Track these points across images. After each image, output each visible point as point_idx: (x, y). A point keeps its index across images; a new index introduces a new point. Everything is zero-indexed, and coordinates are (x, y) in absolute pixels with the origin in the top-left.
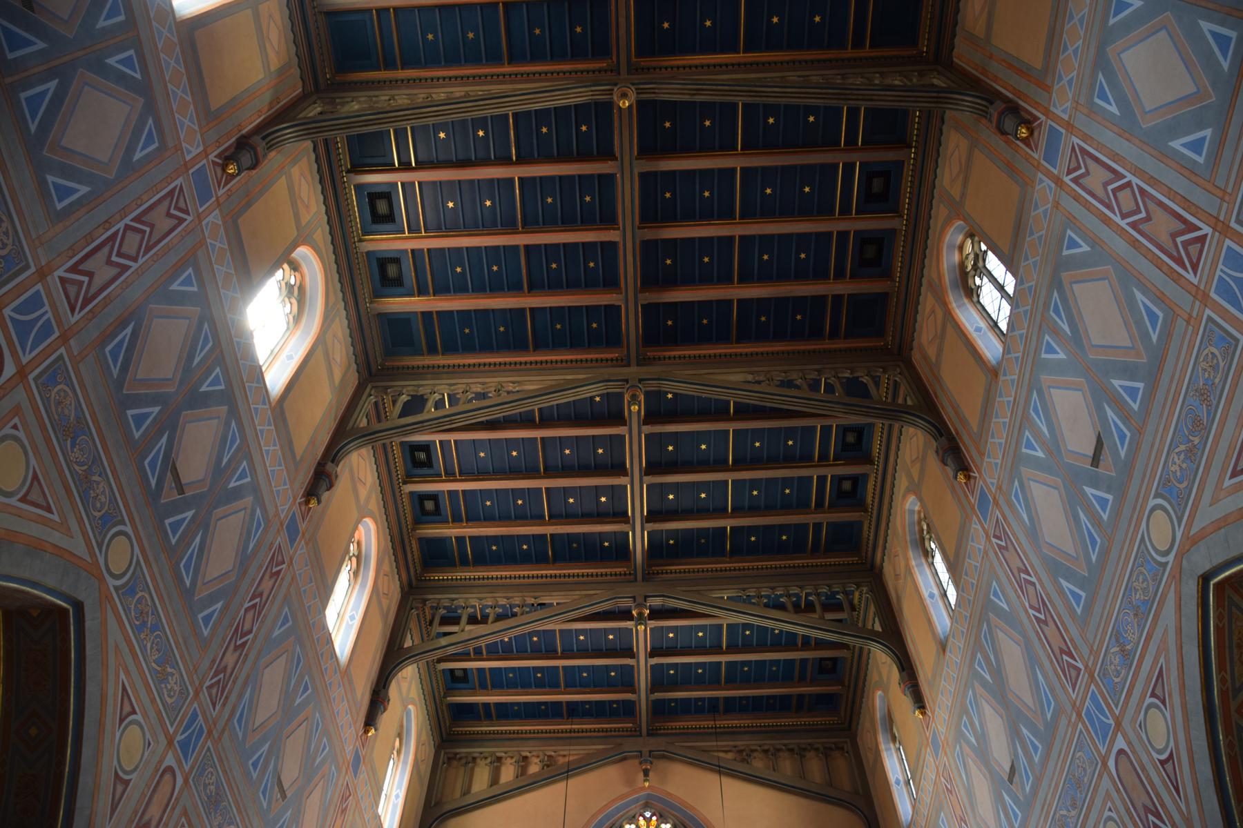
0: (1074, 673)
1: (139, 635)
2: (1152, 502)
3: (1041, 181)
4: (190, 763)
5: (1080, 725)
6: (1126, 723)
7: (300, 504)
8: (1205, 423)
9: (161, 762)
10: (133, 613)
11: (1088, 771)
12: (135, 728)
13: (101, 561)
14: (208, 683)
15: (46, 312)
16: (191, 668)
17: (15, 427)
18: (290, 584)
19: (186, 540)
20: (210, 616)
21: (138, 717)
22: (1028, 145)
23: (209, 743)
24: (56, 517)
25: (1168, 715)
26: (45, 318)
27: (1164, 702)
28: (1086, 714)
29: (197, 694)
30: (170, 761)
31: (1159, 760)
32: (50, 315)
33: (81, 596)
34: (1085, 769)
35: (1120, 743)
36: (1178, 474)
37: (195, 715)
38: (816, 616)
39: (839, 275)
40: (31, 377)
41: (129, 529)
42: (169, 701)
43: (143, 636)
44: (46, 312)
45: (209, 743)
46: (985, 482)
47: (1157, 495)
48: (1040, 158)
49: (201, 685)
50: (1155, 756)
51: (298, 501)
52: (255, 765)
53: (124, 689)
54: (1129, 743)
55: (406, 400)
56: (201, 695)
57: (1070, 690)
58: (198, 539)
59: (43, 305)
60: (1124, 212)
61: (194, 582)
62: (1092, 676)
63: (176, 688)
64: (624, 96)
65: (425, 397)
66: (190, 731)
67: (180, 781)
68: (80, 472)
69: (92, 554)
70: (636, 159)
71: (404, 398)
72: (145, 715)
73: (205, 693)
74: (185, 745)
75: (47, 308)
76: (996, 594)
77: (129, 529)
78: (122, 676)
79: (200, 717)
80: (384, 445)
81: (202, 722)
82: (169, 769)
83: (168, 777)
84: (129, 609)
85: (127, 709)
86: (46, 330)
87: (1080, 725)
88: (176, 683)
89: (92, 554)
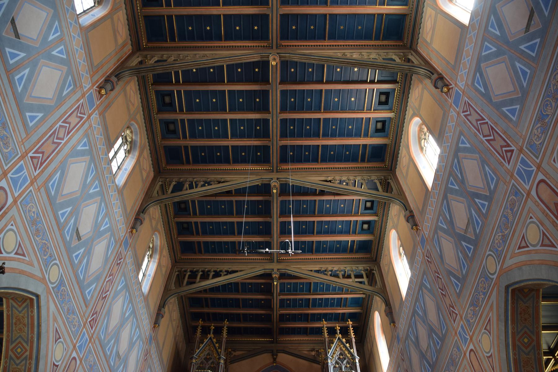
0: (455, 315)
1: (62, 305)
2: (488, 253)
3: (452, 112)
4: (82, 355)
5: (456, 337)
6: (474, 339)
7: (129, 232)
8: (509, 226)
9: (71, 355)
10: (59, 297)
11: (458, 356)
12: (61, 344)
13: (47, 277)
14: (89, 320)
15: (25, 172)
16: (82, 314)
17: (12, 225)
18: (124, 269)
19: (80, 262)
20: (90, 291)
21: (62, 340)
22: (447, 95)
23: (90, 344)
24: (27, 259)
25: (491, 338)
26: (25, 174)
27: (490, 333)
28: (459, 333)
29: (84, 325)
30: (74, 354)
31: (487, 356)
32: (26, 173)
33: (39, 293)
34: (457, 355)
35: (471, 347)
36: (498, 244)
37: (84, 334)
38: (350, 280)
39: (366, 135)
40: (19, 202)
41: (57, 262)
42: (73, 330)
43: (63, 305)
44: (25, 172)
45: (90, 344)
46: (424, 232)
47: (490, 250)
48: (451, 102)
49: (87, 321)
50: (485, 354)
51: (129, 231)
52: (109, 350)
53: (56, 329)
54: (475, 348)
55: (174, 184)
56: (87, 325)
57: (453, 322)
58: (85, 260)
59: (24, 170)
60: (487, 125)
61: (84, 277)
62: (461, 317)
63: (77, 324)
64: (274, 59)
65: (183, 183)
66: (82, 341)
67: (78, 362)
68: (38, 240)
69: (43, 273)
70: (279, 84)
71: (174, 183)
72: (65, 340)
73: (88, 324)
74: (80, 347)
75: (25, 170)
76: (425, 281)
77: (57, 262)
78: (56, 325)
79: (86, 334)
80: (165, 204)
81: (87, 336)
82: (74, 358)
83: (74, 361)
84: (58, 295)
85: (58, 337)
86: (25, 180)
87: (456, 337)
88: (76, 322)
89: (43, 273)
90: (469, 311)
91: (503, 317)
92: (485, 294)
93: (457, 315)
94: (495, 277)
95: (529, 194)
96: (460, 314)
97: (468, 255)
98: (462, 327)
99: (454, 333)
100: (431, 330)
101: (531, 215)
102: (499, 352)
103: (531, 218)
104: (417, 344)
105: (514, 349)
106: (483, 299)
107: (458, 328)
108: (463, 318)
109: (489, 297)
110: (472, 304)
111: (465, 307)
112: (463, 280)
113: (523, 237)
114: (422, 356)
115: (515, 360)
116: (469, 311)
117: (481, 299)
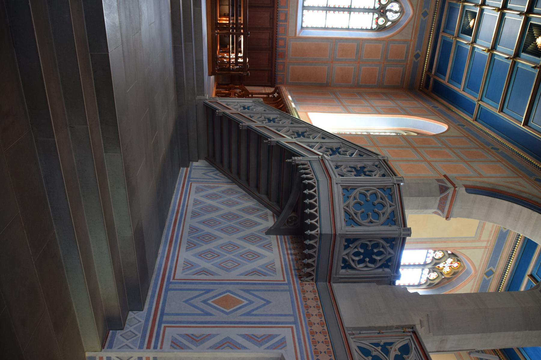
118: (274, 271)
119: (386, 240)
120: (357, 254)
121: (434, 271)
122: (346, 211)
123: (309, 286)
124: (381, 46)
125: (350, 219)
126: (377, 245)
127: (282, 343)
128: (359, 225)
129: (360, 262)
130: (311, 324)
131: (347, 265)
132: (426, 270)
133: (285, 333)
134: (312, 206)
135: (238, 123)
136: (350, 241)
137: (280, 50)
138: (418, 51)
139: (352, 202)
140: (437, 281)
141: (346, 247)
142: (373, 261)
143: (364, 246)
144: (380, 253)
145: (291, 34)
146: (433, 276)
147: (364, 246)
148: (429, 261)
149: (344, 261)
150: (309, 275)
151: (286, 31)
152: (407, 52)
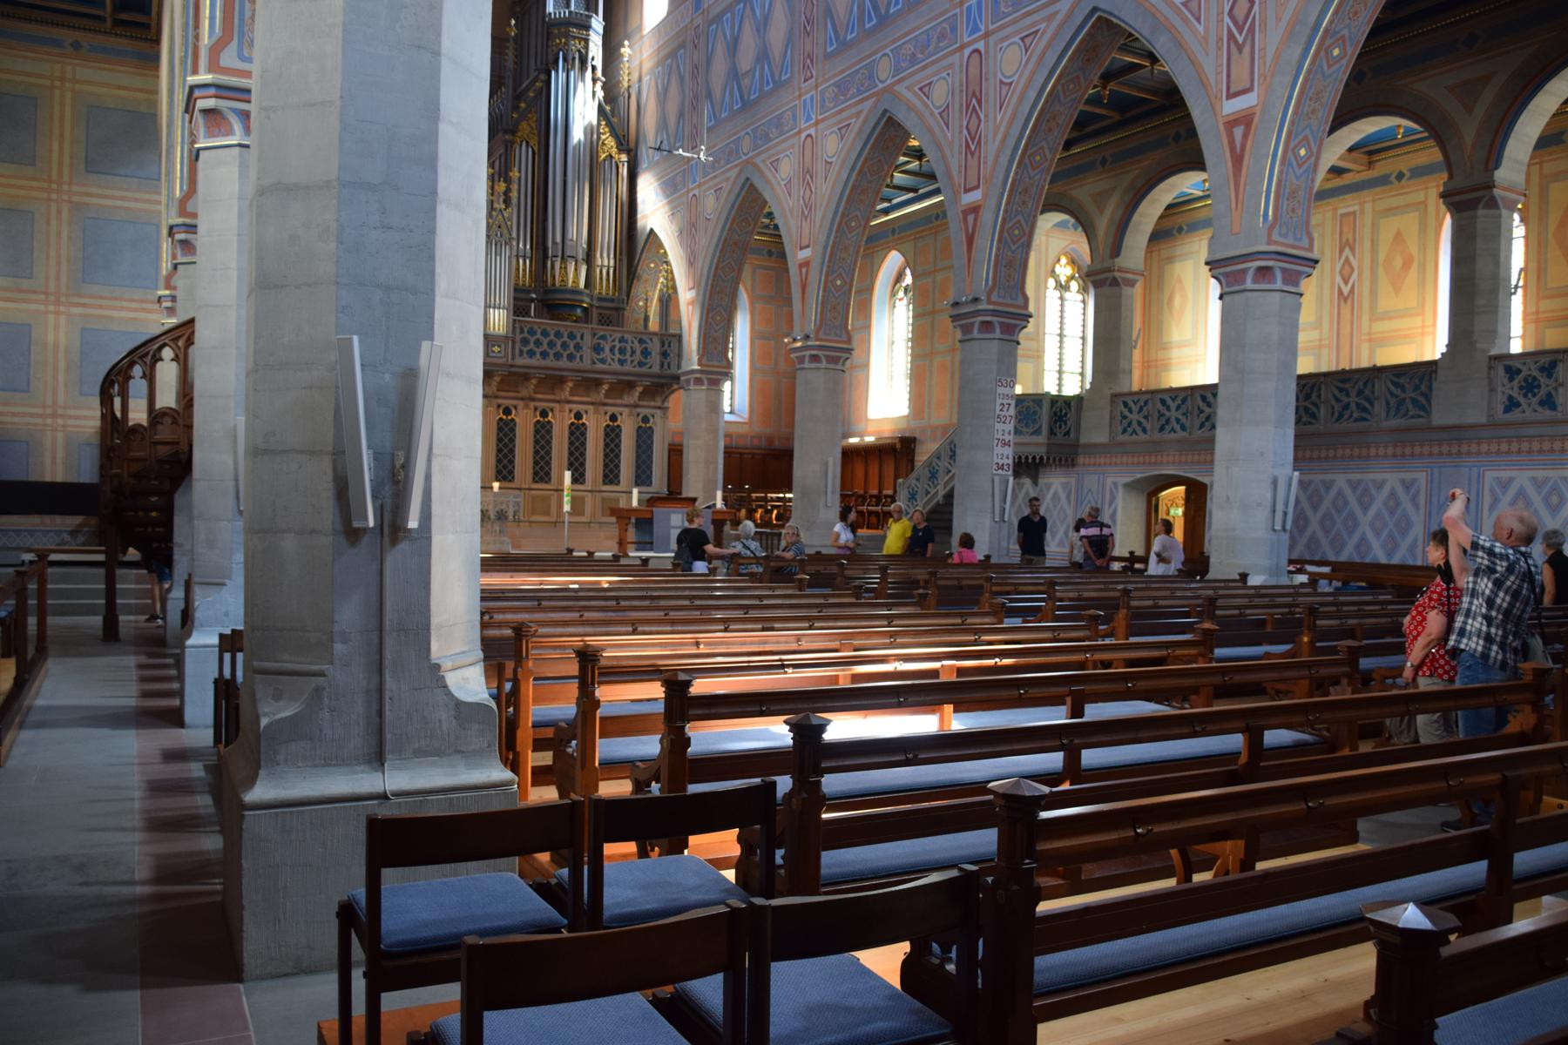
90: (830, 89)
91: (865, 136)
92: (860, 92)
93: (812, 77)
94: (881, 86)
95: (962, 47)
96: (817, 79)
97: (864, 26)
98: (812, 97)
99: (797, 94)
100: (763, 55)
101: (950, 71)
102: (841, 167)
103: (948, 74)
104: (733, 46)
105: (859, 174)
106: (853, 96)
107: (807, 93)
108: (820, 89)
109: (861, 101)
110: (838, 85)
111: (829, 80)
112: (844, 46)
113: (930, 84)
114: (734, 74)
115: (854, 186)
116: (830, 89)
117: (851, 92)
118: (1068, 483)
119: (1052, 407)
120: (1060, 427)
121: (1069, 287)
122: (1032, 434)
123: (1081, 460)
124: (759, 305)
125: (1037, 432)
126: (1055, 413)
127: (1115, 484)
128: (1041, 426)
129: (1066, 424)
130: (1105, 464)
131: (1068, 433)
132: (1067, 295)
133: (1109, 481)
134: (1027, 458)
135: (938, 504)
136: (1052, 433)
137: (764, 443)
138: (765, 252)
139: (1024, 430)
140: (1081, 282)
141: (1055, 434)
142: (1066, 414)
143: (1055, 422)
144: (1061, 410)
145: (744, 430)
146: (1074, 285)
147: (1055, 422)
148: (1058, 294)
149: (1065, 435)
150: (1073, 460)
151: (741, 436)
152: (765, 268)
